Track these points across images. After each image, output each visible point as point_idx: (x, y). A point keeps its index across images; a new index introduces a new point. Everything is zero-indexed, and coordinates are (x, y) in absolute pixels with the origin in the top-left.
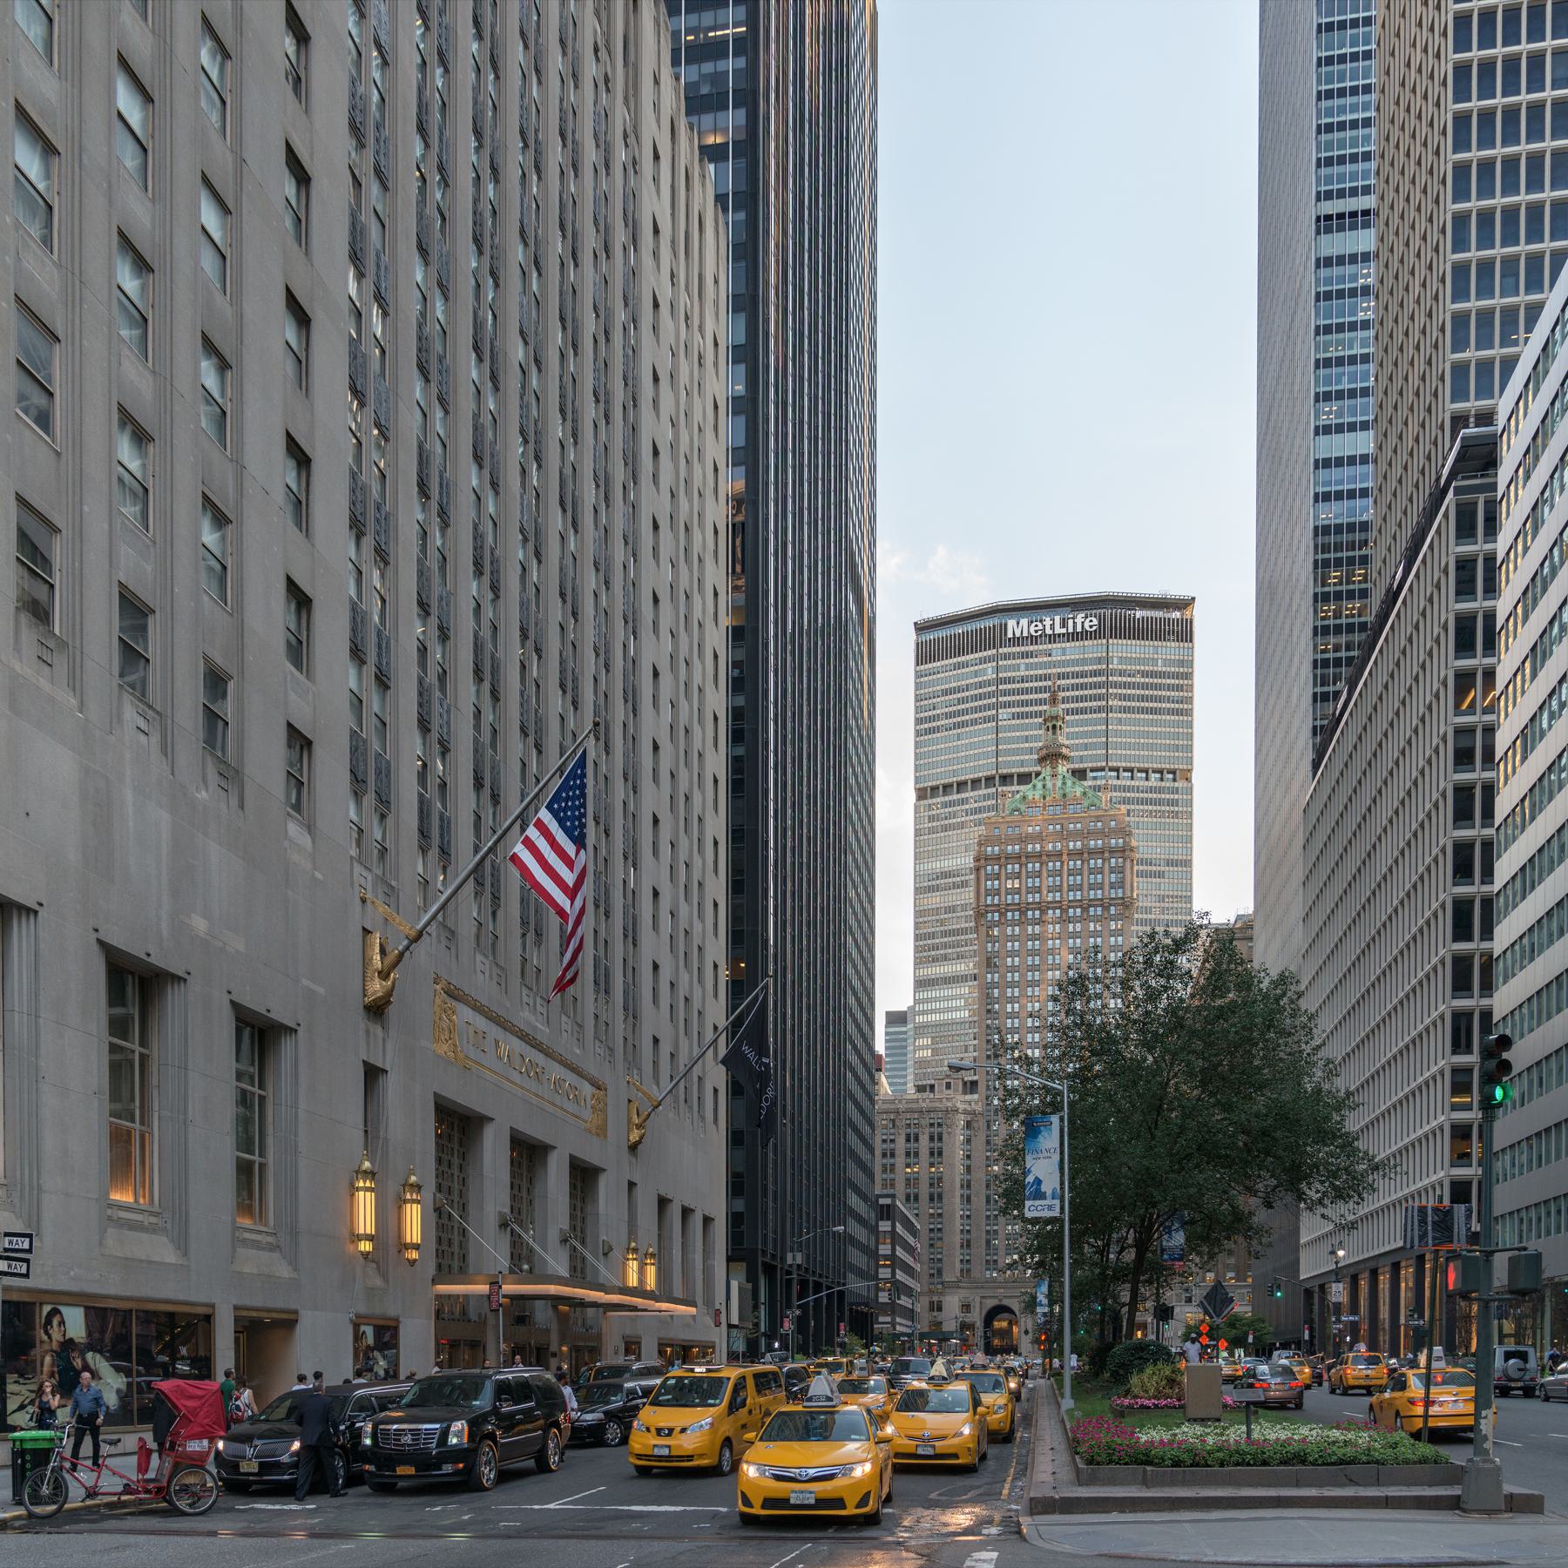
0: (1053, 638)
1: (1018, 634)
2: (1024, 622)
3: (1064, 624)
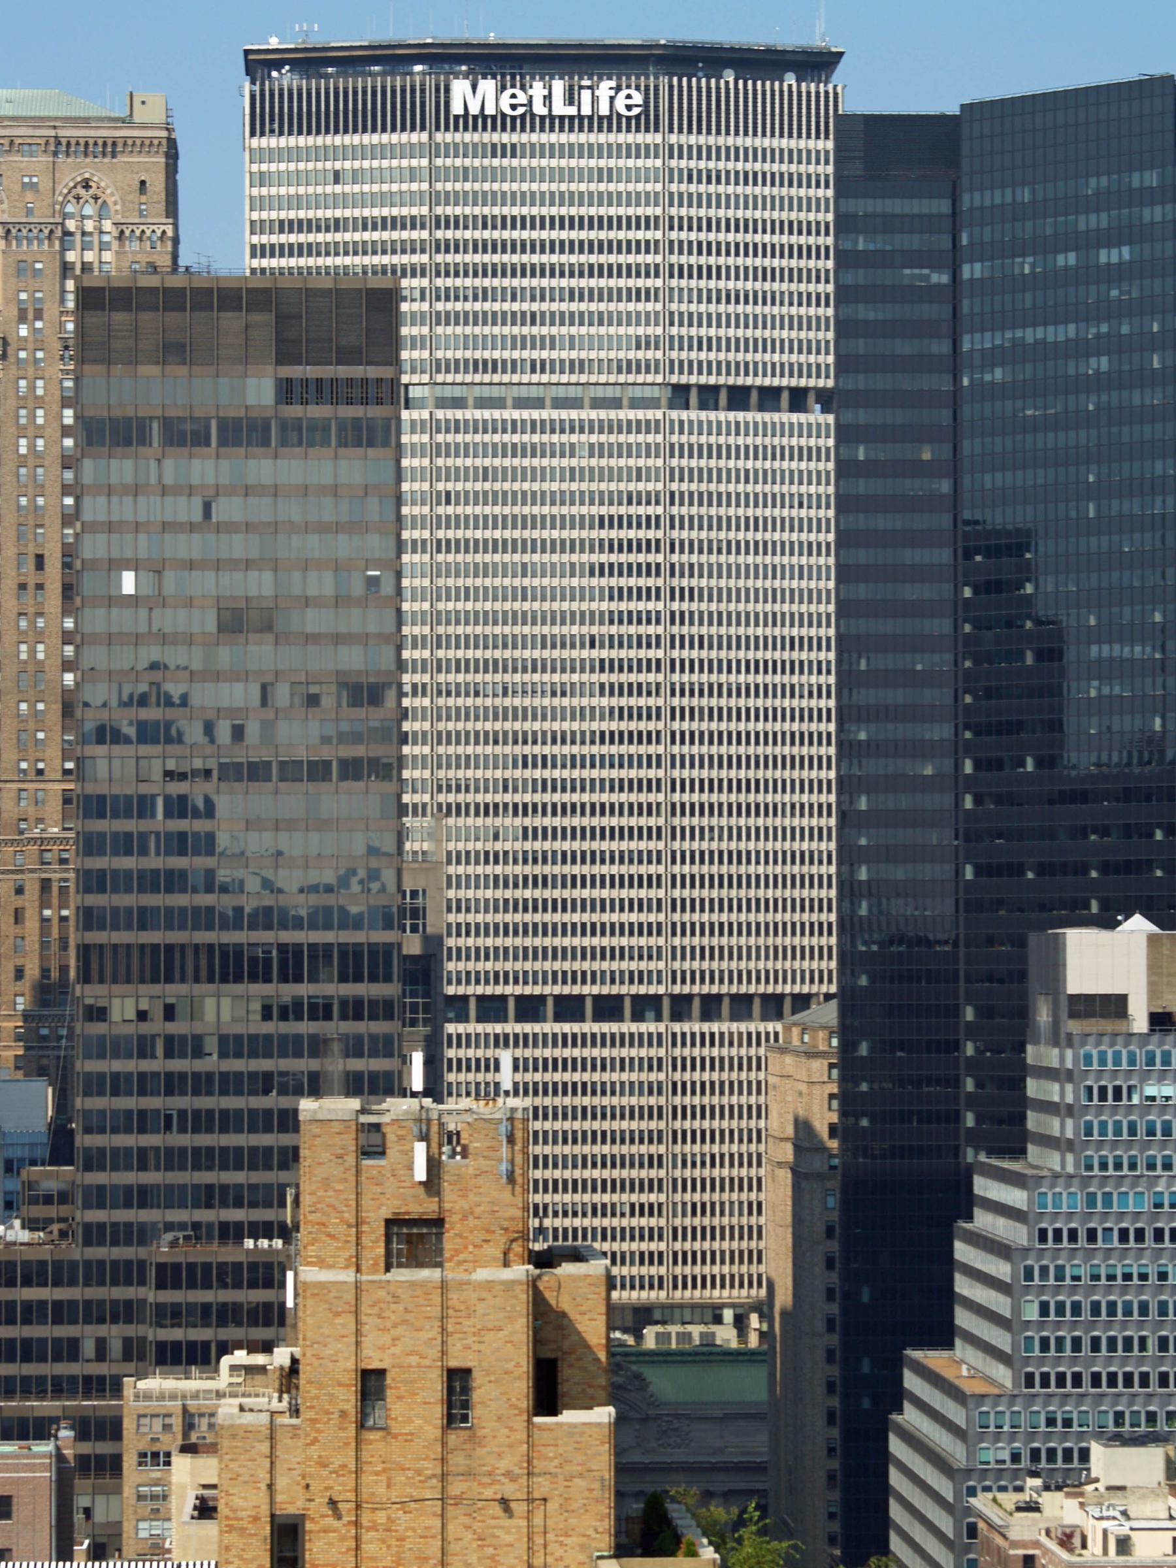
0: (551, 122)
1: (474, 110)
2: (488, 86)
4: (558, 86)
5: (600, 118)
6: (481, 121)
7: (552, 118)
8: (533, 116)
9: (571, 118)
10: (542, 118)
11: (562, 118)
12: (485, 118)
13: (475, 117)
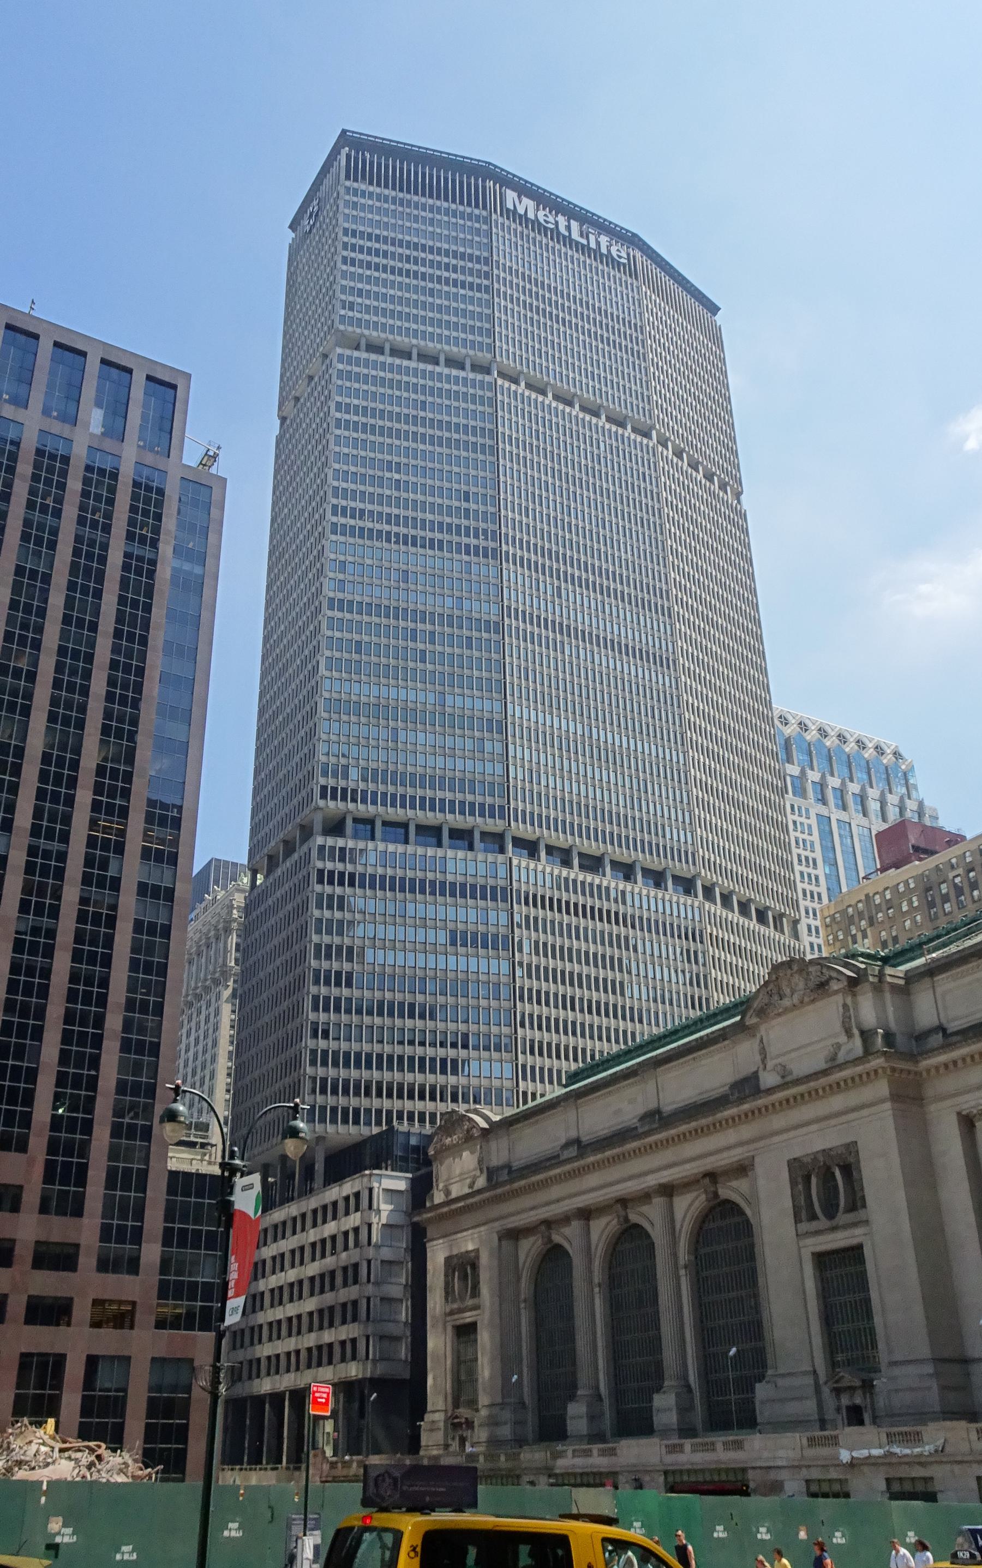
5: (601, 255)
7: (571, 240)
8: (559, 233)
11: (577, 243)
12: (527, 219)
13: (520, 216)
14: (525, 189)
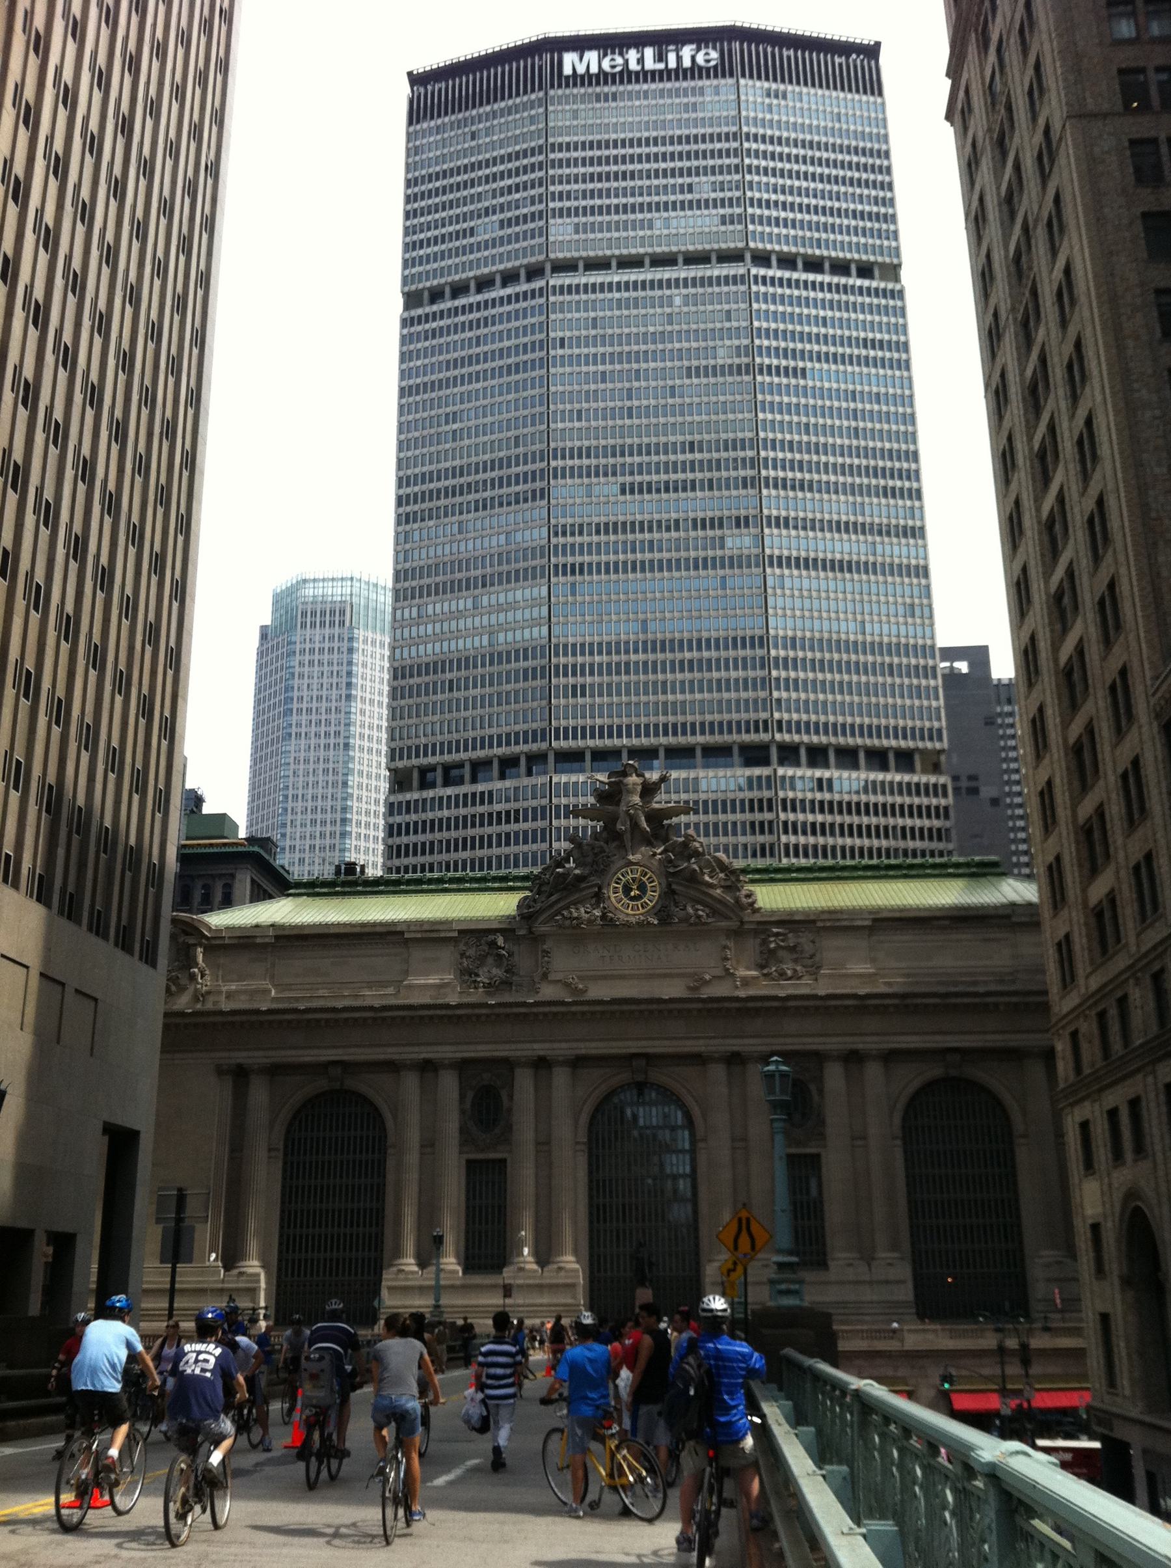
1: (581, 70)
2: (592, 56)
3: (660, 57)
4: (649, 52)
6: (587, 79)
7: (645, 73)
8: (630, 73)
9: (661, 72)
10: (637, 73)
11: (653, 72)
12: (590, 76)
13: (582, 77)
14: (580, 44)
